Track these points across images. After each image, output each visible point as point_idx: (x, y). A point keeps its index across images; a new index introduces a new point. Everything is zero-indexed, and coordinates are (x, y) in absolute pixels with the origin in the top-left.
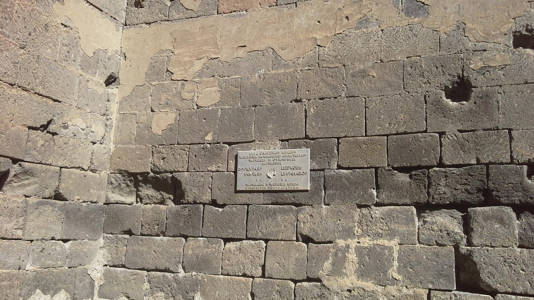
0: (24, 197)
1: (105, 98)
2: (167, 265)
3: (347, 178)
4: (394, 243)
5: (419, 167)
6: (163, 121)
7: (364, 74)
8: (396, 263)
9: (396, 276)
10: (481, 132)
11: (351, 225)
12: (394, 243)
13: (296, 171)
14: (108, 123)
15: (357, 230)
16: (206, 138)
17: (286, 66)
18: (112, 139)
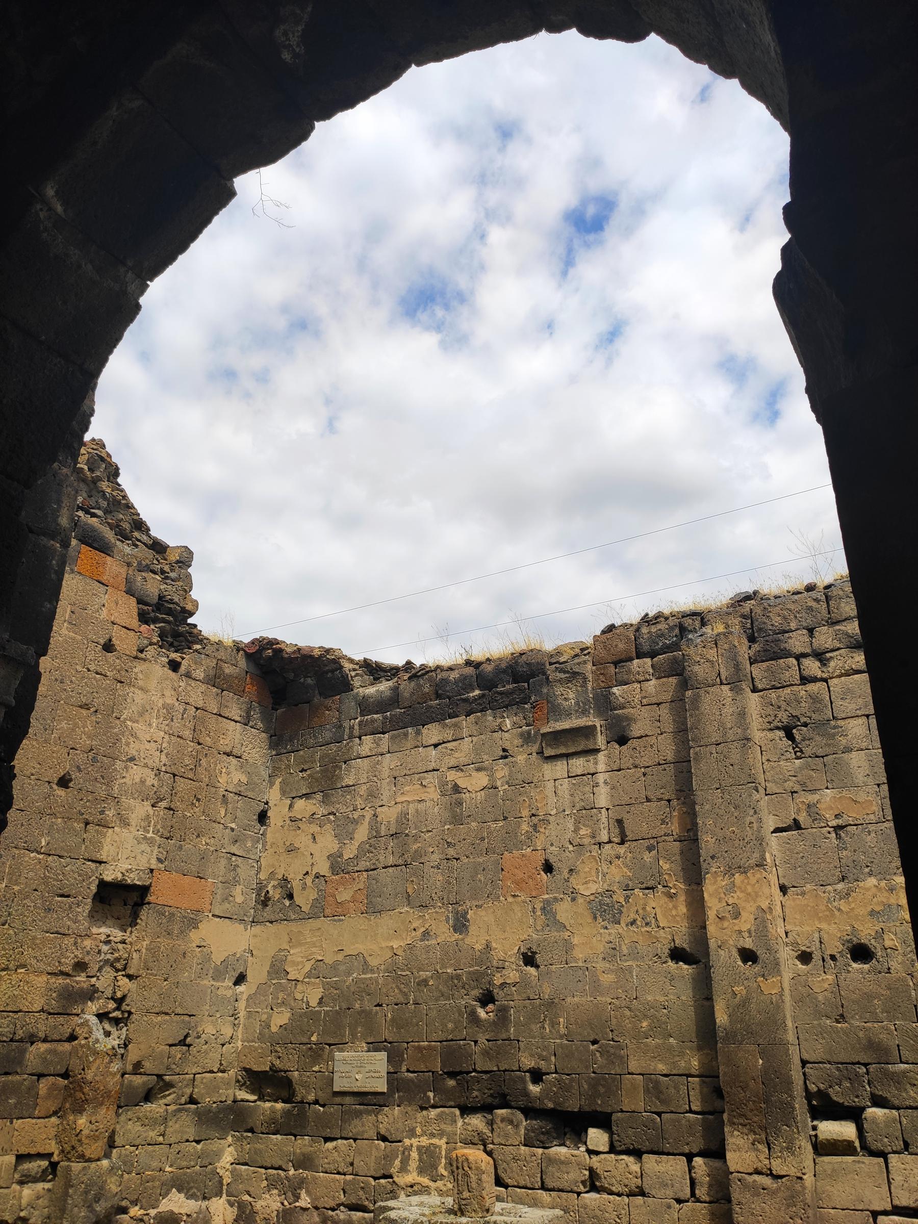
0: (165, 1107)
1: (232, 999)
2: (280, 1163)
3: (411, 1080)
4: (442, 1142)
5: (461, 1073)
6: (281, 1018)
7: (425, 982)
8: (443, 1161)
9: (445, 1173)
10: (501, 1042)
11: (414, 1125)
12: (442, 1142)
13: (376, 1075)
14: (236, 1022)
15: (419, 1131)
16: (312, 1039)
17: (372, 971)
18: (240, 1037)
